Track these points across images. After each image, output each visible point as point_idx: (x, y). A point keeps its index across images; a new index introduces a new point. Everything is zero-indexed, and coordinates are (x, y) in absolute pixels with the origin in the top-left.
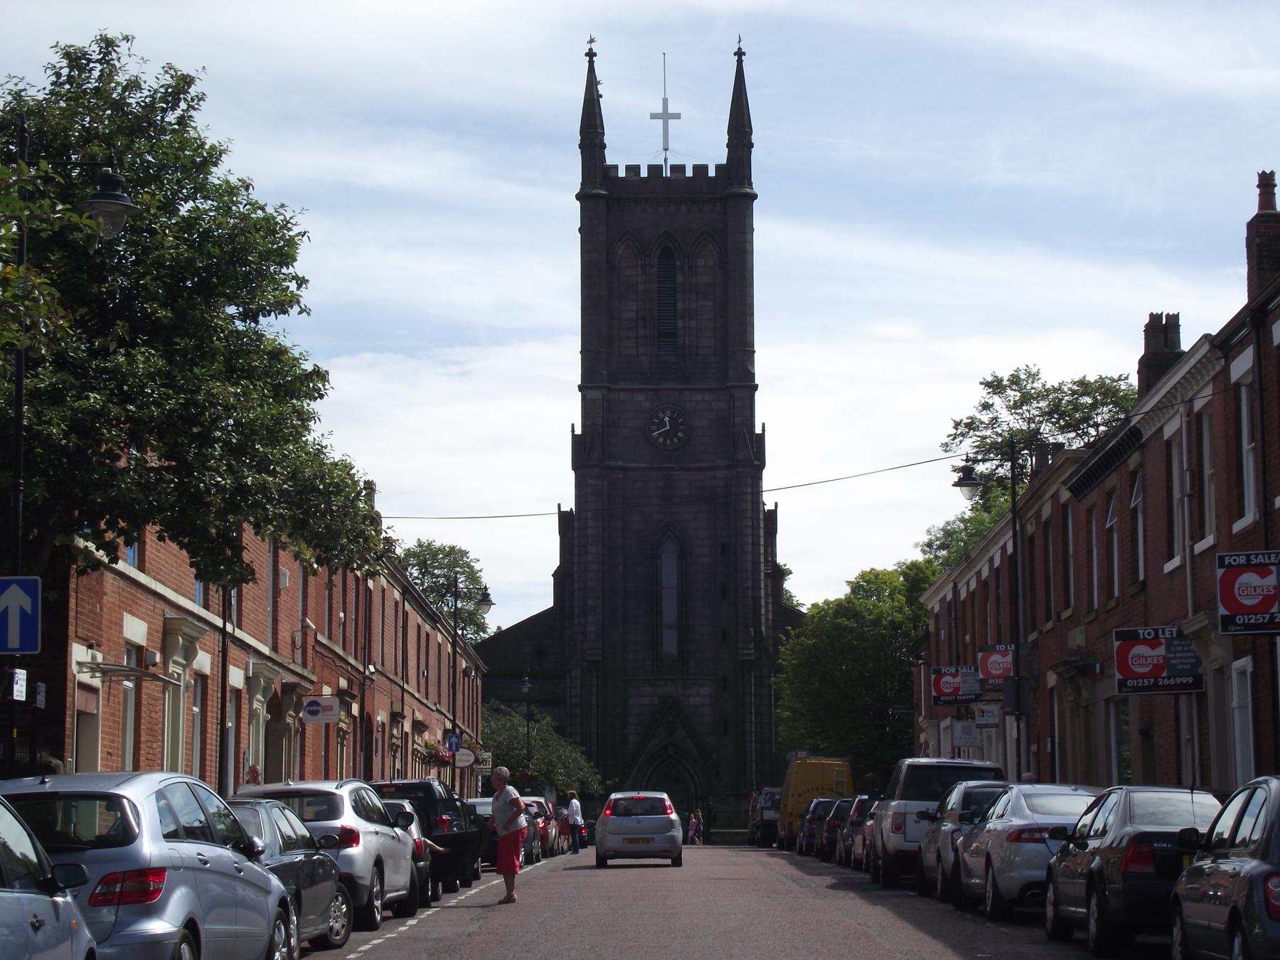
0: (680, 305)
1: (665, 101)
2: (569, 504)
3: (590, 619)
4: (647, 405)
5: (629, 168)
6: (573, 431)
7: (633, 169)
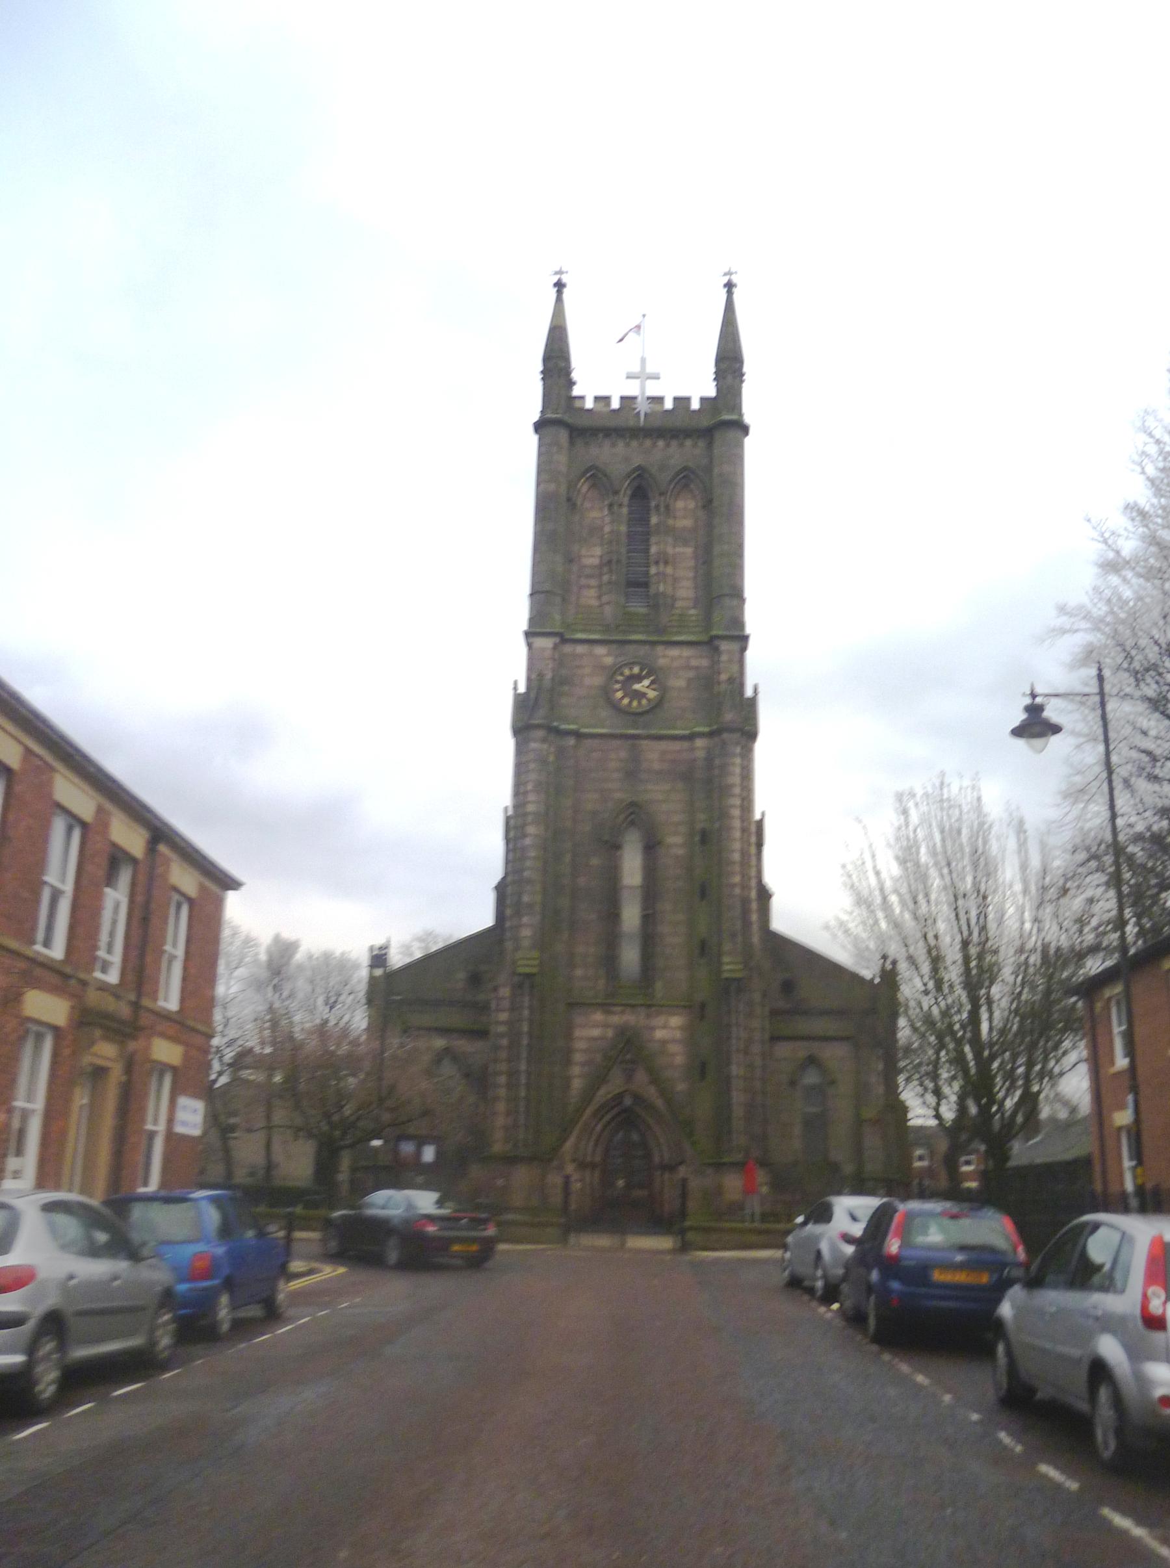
0: (653, 550)
1: (643, 361)
4: (609, 660)
5: (597, 399)
7: (604, 400)
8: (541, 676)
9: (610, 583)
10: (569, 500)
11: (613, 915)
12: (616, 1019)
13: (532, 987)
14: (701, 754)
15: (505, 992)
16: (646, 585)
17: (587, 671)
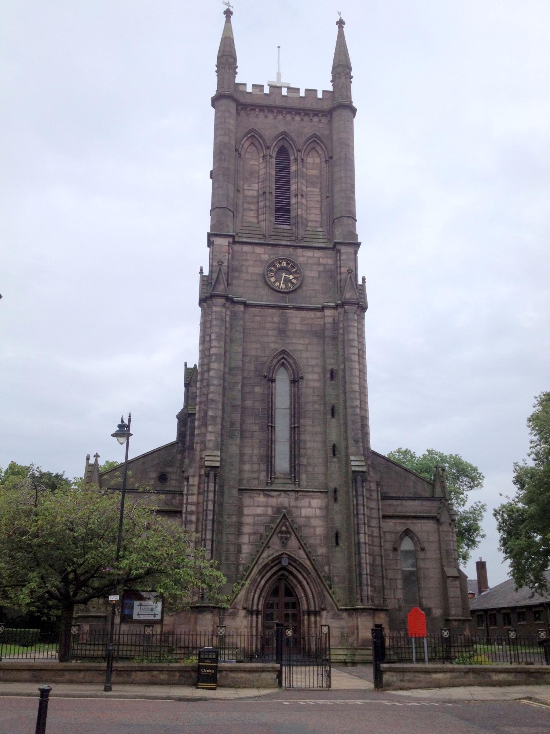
0: (293, 187)
1: (279, 75)
2: (194, 360)
3: (210, 428)
4: (266, 257)
6: (201, 272)
8: (221, 263)
9: (265, 206)
10: (236, 150)
11: (271, 428)
12: (274, 501)
13: (215, 475)
14: (329, 320)
15: (194, 481)
16: (288, 211)
17: (251, 263)
